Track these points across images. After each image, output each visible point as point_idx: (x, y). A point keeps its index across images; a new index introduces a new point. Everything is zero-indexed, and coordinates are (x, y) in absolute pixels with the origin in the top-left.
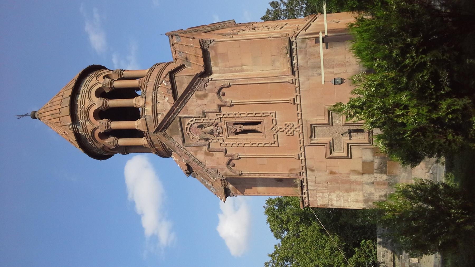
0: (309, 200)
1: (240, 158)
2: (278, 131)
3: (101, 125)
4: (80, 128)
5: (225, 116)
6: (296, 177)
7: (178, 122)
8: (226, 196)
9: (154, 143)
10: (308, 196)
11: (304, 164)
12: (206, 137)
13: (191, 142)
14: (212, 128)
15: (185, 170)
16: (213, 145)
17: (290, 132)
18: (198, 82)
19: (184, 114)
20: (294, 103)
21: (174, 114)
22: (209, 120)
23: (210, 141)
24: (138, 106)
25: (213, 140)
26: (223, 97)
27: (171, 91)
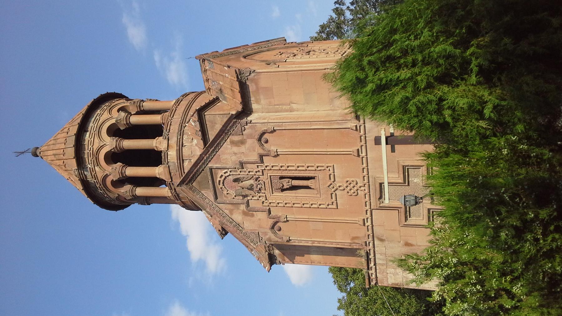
0: (376, 277)
1: (287, 221)
3: (114, 171)
4: (88, 174)
6: (361, 247)
7: (209, 174)
8: (271, 264)
9: (180, 195)
11: (370, 232)
12: (244, 194)
13: (225, 198)
14: (252, 182)
15: (219, 230)
16: (252, 204)
17: (352, 191)
18: (233, 125)
19: (216, 163)
20: (359, 156)
21: (204, 163)
22: (247, 173)
23: (249, 198)
24: (160, 150)
25: (253, 197)
26: (265, 145)
27: (200, 133)
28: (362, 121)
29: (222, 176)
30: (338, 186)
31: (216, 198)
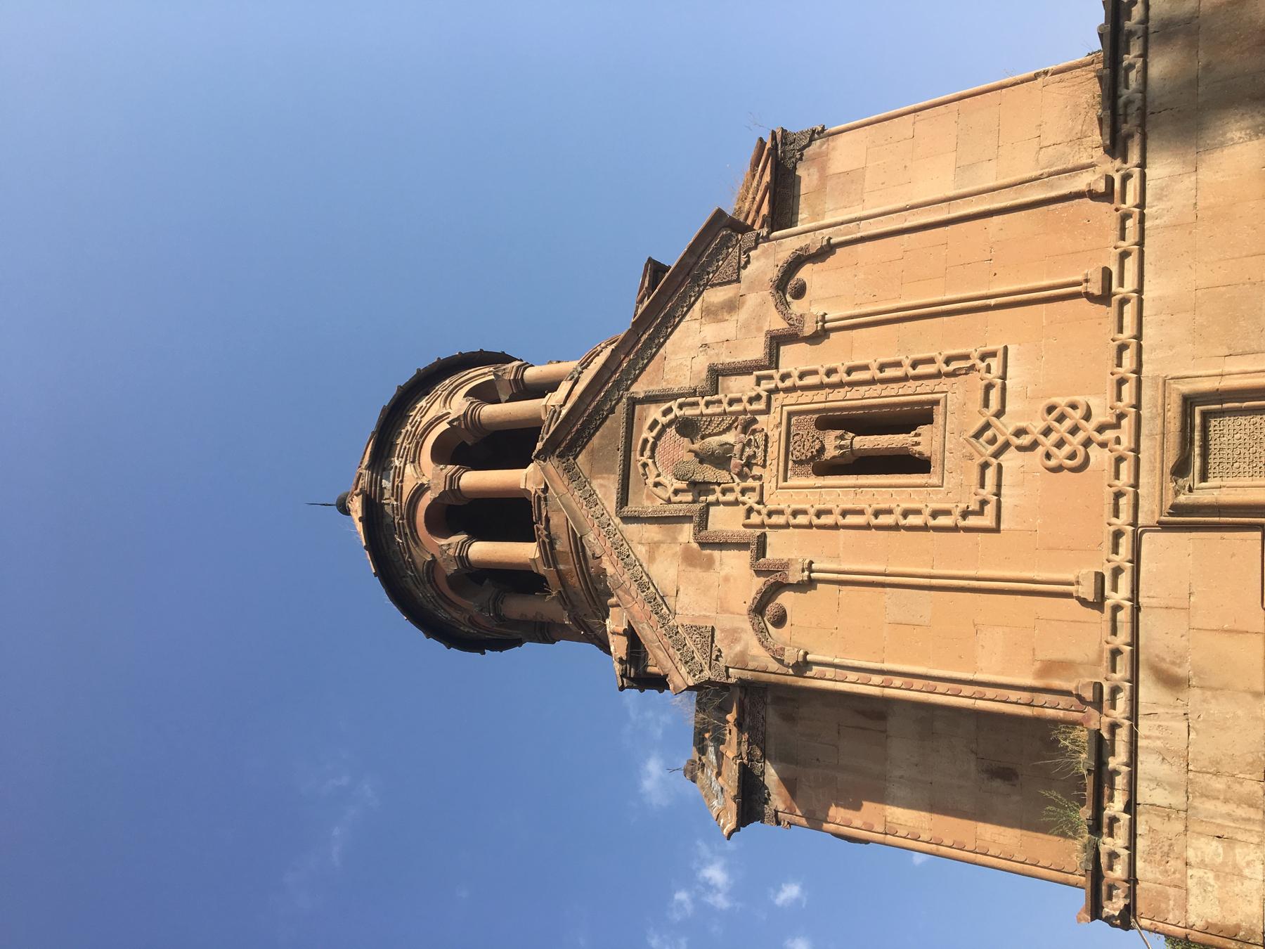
0: (1132, 879)
2: (1007, 445)
4: (386, 484)
5: (788, 383)
6: (1076, 716)
9: (558, 547)
10: (1132, 846)
11: (1123, 636)
12: (699, 478)
13: (647, 503)
14: (730, 437)
17: (1067, 449)
18: (718, 250)
19: (651, 383)
21: (617, 384)
23: (711, 498)
25: (724, 492)
28: (1134, 157)
29: (655, 423)
30: (1011, 429)
31: (623, 500)
